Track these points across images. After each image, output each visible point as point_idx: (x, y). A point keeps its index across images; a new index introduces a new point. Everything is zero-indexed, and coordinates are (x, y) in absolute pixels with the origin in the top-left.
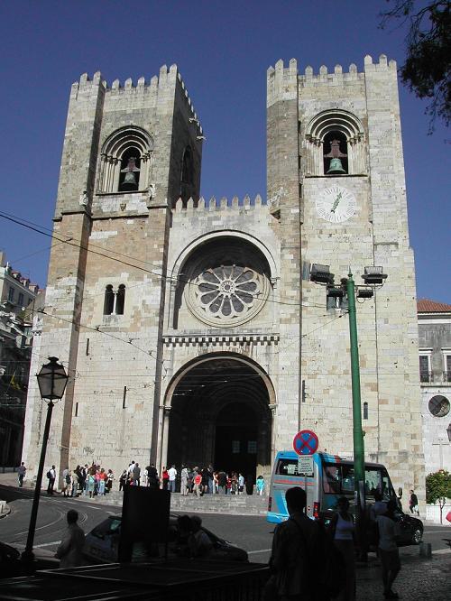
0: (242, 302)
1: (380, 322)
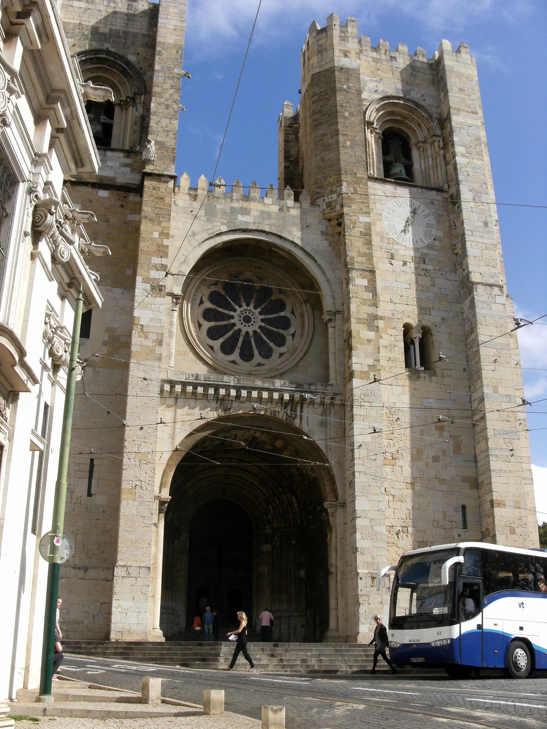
0: (271, 344)
1: (487, 390)
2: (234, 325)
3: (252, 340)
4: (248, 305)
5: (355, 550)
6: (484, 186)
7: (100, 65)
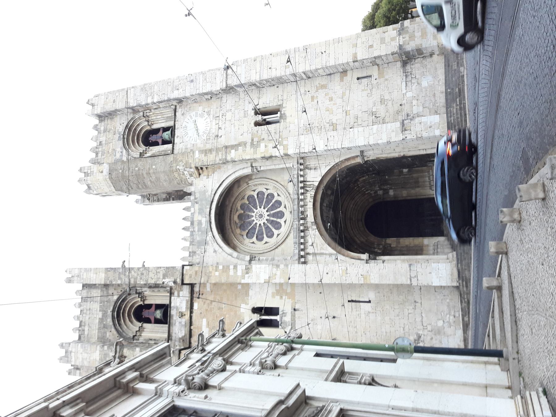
0: (273, 201)
2: (264, 223)
3: (272, 212)
4: (253, 216)
5: (389, 143)
6: (169, 84)
7: (121, 315)
